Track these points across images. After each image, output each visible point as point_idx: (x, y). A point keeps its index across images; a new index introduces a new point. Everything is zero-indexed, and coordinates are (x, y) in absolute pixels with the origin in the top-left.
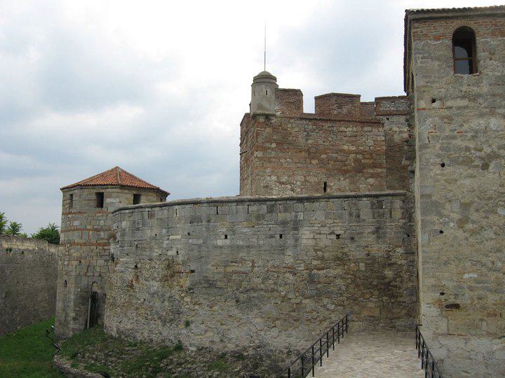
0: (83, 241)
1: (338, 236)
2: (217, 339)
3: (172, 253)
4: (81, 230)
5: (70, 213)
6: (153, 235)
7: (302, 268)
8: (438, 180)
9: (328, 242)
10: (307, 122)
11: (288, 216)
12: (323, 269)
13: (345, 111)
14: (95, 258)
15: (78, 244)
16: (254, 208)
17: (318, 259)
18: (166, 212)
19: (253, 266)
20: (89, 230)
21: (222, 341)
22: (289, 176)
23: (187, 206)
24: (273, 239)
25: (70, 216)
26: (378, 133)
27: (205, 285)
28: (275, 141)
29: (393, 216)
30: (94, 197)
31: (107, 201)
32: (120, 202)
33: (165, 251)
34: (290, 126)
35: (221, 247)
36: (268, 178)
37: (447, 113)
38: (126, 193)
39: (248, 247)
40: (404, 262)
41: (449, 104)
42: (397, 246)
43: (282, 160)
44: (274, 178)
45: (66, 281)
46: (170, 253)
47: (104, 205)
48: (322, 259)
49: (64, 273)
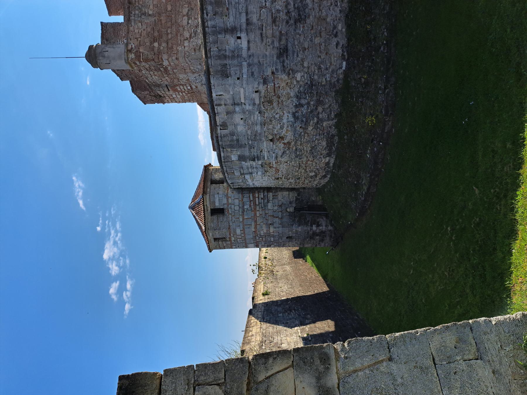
0: (253, 224)
2: (334, 41)
4: (244, 225)
15: (256, 228)
16: (209, 8)
20: (243, 219)
21: (336, 36)
23: (212, 82)
25: (233, 239)
27: (285, 56)
30: (215, 217)
31: (217, 205)
32: (218, 193)
34: (136, 31)
35: (249, 42)
36: (186, 49)
38: (210, 189)
43: (170, 36)
44: (186, 43)
46: (257, 102)
47: (222, 207)
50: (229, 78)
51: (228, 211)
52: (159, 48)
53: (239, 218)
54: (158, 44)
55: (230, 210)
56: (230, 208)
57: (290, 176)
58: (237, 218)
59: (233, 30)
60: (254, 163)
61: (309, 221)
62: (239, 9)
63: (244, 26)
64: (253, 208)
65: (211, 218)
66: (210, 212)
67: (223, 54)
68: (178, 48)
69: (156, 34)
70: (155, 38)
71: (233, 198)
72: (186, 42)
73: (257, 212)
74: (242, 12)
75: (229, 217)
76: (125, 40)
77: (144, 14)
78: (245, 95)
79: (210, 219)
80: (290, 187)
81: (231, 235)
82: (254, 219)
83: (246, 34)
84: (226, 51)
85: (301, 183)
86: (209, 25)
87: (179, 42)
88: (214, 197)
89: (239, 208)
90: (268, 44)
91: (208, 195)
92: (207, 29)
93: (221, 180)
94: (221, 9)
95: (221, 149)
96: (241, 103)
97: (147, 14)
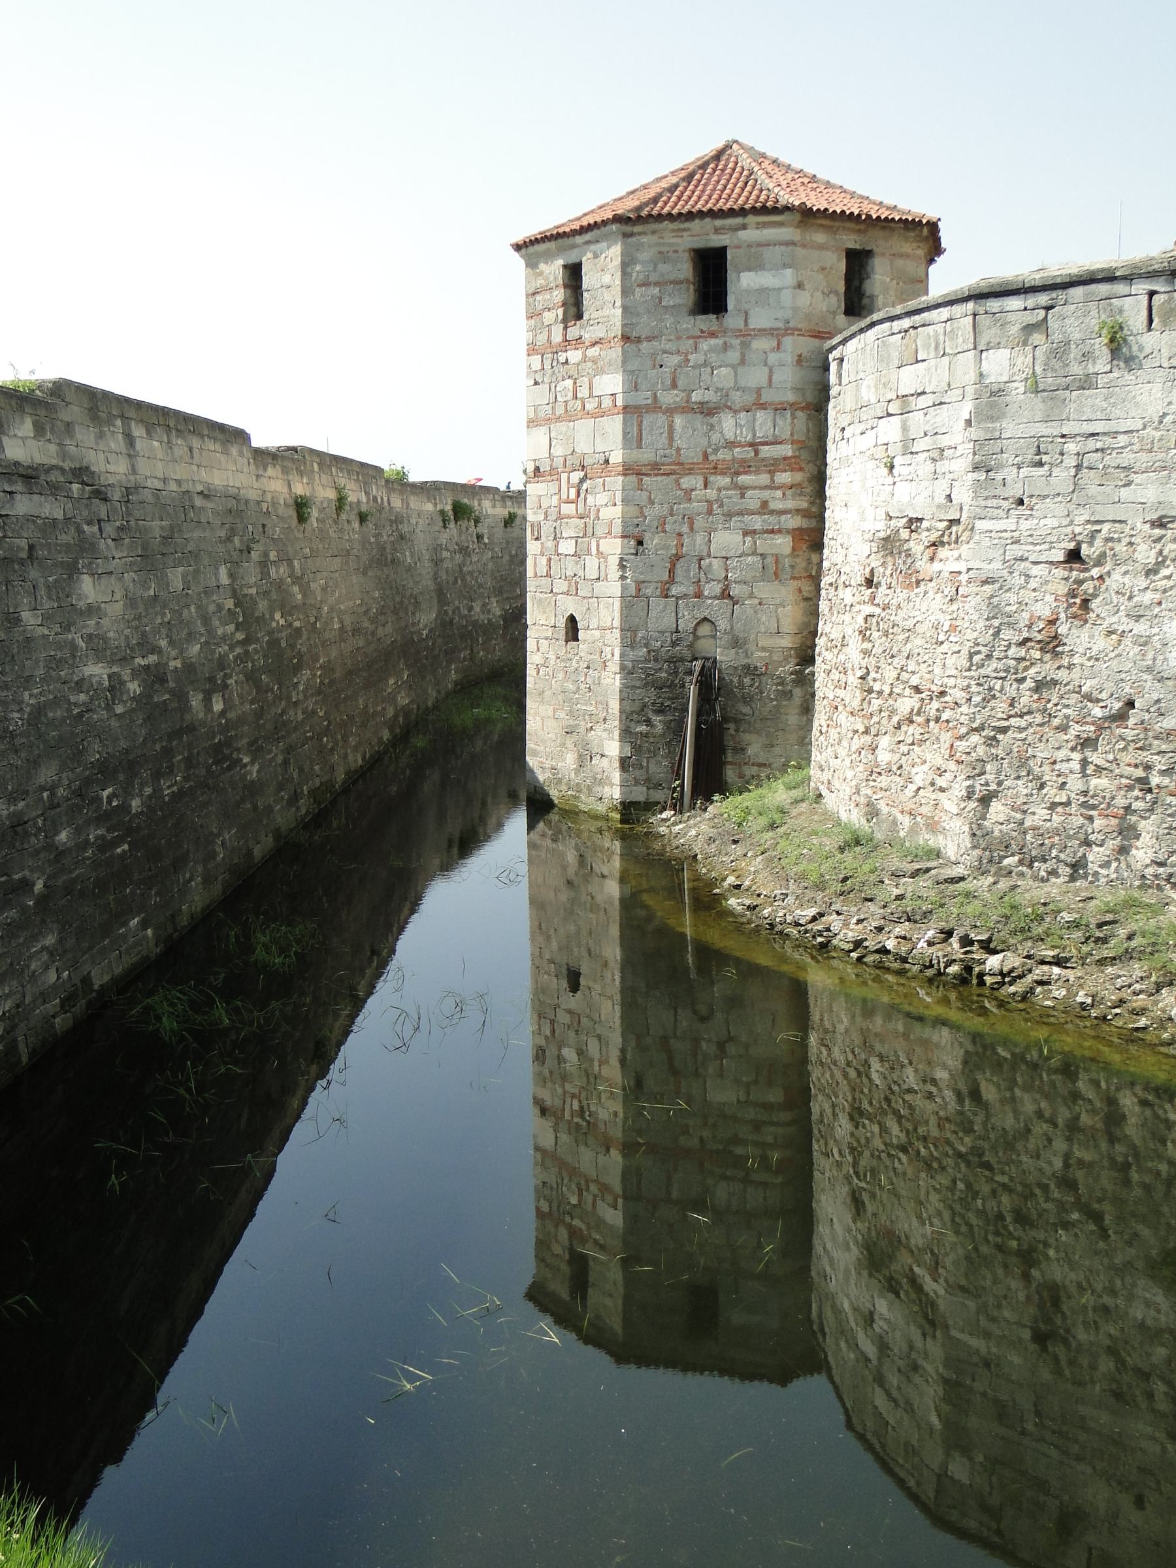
14: (699, 522)
20: (670, 411)
25: (574, 356)
30: (685, 269)
32: (800, 286)
38: (821, 247)
45: (572, 620)
51: (713, 335)
53: (674, 385)
55: (718, 342)
56: (725, 343)
57: (879, 643)
60: (960, 465)
61: (648, 722)
65: (681, 249)
71: (773, 358)
80: (821, 642)
81: (593, 344)
85: (841, 693)
88: (785, 266)
93: (865, 301)
95: (1043, 299)
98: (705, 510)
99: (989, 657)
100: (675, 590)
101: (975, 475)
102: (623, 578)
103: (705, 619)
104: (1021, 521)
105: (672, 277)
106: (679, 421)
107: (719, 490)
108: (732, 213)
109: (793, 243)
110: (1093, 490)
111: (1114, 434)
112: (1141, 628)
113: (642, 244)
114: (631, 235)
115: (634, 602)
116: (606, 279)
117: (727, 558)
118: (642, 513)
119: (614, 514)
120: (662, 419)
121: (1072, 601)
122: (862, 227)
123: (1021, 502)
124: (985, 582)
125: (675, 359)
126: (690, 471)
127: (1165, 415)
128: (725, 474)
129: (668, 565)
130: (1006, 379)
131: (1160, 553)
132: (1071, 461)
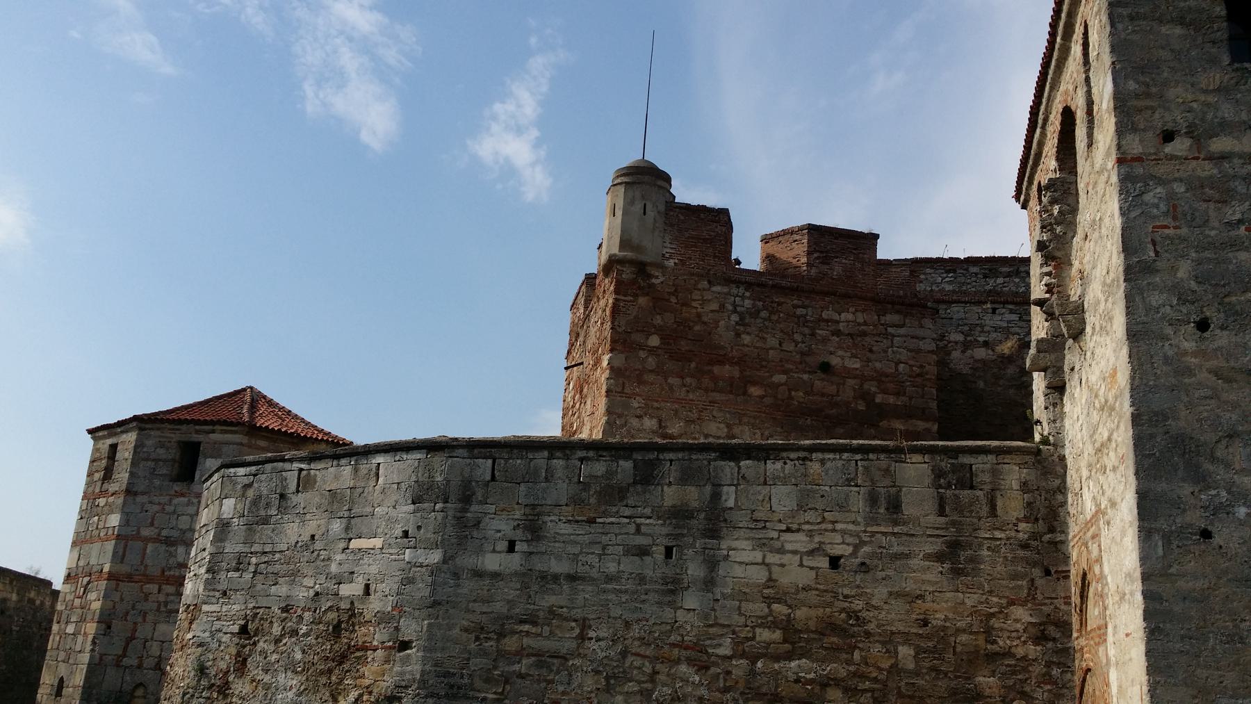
1: (835, 562)
3: (350, 590)
5: (103, 493)
6: (306, 537)
7: (728, 652)
8: (1189, 371)
9: (806, 577)
10: (741, 290)
11: (694, 496)
12: (789, 657)
13: (837, 270)
14: (150, 617)
16: (599, 468)
17: (774, 625)
18: (347, 471)
19: (582, 637)
20: (147, 540)
22: (689, 422)
24: (648, 559)
26: (920, 332)
28: (659, 330)
29: (999, 512)
30: (174, 453)
33: (331, 586)
35: (496, 576)
36: (635, 422)
37: (1207, 170)
39: (572, 578)
40: (1032, 650)
41: (1220, 144)
42: (1012, 603)
46: (346, 590)
48: (787, 626)
49: (62, 655)
50: (412, 507)
51: (183, 495)
52: (642, 347)
53: (152, 524)
54: (654, 347)
56: (189, 500)
58: (153, 519)
59: (533, 528)
62: (588, 553)
63: (539, 565)
64: (172, 573)
65: (174, 440)
66: (192, 439)
67: (474, 494)
68: (637, 398)
69: (684, 345)
70: (671, 341)
72: (654, 421)
73: (157, 587)
74: (577, 562)
75: (162, 495)
76: (675, 263)
77: (742, 322)
78: (367, 551)
79: (170, 438)
81: (112, 495)
82: (137, 573)
83: (518, 568)
84: (481, 503)
86: (555, 461)
87: (656, 405)
89: (181, 530)
90: (482, 636)
91: (245, 440)
92: (546, 454)
94: (592, 500)
95: (254, 468)
96: (350, 540)
97: (742, 328)
98: (155, 608)
99: (193, 696)
100: (126, 661)
101: (206, 575)
102: (92, 650)
103: (141, 684)
104: (224, 606)
105: (164, 457)
106: (150, 547)
107: (168, 595)
108: (205, 423)
109: (241, 444)
110: (259, 587)
111: (273, 553)
112: (267, 678)
113: (150, 435)
114: (145, 429)
115: (93, 669)
116: (127, 455)
117: (163, 642)
118: (114, 607)
119: (96, 605)
120: (140, 544)
121: (238, 659)
122: (295, 441)
123: (225, 593)
124: (200, 645)
125: (156, 508)
126: (150, 580)
127: (297, 542)
128: (173, 584)
129: (123, 644)
130: (231, 516)
131: (284, 627)
132: (252, 569)
